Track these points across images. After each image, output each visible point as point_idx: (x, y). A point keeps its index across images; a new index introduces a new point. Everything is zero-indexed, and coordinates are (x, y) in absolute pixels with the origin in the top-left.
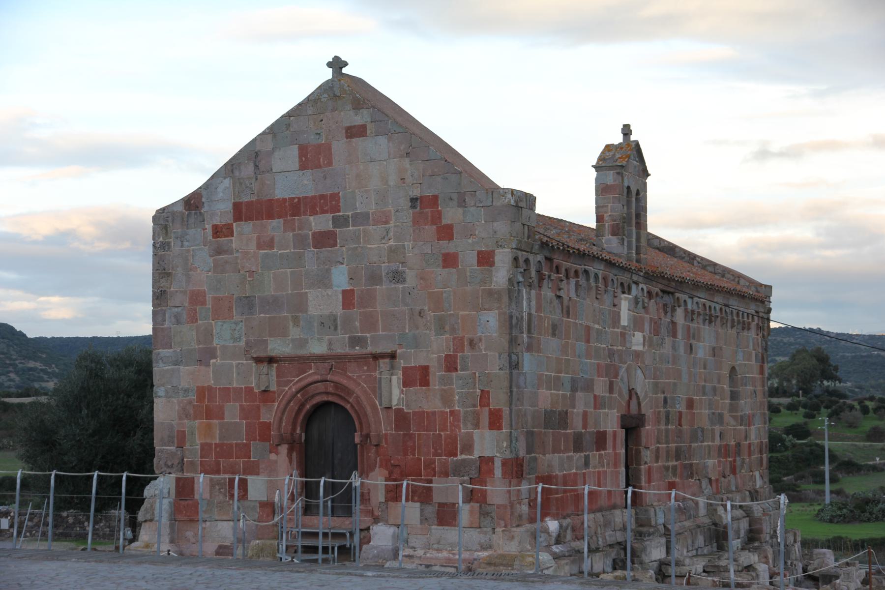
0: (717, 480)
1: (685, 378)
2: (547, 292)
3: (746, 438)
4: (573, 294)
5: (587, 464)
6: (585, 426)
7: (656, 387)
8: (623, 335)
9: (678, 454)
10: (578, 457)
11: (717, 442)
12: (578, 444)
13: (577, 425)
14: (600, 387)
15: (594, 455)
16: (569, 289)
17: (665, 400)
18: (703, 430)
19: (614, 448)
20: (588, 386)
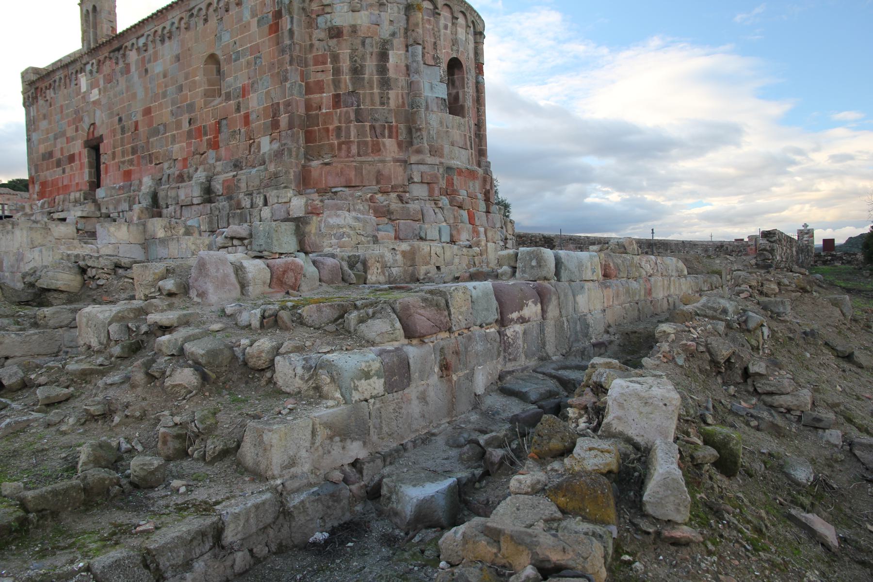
0: (185, 160)
1: (141, 94)
2: (41, 102)
3: (238, 109)
4: (53, 95)
5: (64, 172)
6: (62, 154)
7: (111, 115)
8: (83, 97)
9: (134, 151)
10: (60, 170)
11: (186, 127)
12: (59, 164)
13: (58, 155)
14: (70, 132)
15: (68, 168)
16: (50, 94)
17: (120, 120)
18: (165, 125)
19: (80, 160)
20: (63, 134)
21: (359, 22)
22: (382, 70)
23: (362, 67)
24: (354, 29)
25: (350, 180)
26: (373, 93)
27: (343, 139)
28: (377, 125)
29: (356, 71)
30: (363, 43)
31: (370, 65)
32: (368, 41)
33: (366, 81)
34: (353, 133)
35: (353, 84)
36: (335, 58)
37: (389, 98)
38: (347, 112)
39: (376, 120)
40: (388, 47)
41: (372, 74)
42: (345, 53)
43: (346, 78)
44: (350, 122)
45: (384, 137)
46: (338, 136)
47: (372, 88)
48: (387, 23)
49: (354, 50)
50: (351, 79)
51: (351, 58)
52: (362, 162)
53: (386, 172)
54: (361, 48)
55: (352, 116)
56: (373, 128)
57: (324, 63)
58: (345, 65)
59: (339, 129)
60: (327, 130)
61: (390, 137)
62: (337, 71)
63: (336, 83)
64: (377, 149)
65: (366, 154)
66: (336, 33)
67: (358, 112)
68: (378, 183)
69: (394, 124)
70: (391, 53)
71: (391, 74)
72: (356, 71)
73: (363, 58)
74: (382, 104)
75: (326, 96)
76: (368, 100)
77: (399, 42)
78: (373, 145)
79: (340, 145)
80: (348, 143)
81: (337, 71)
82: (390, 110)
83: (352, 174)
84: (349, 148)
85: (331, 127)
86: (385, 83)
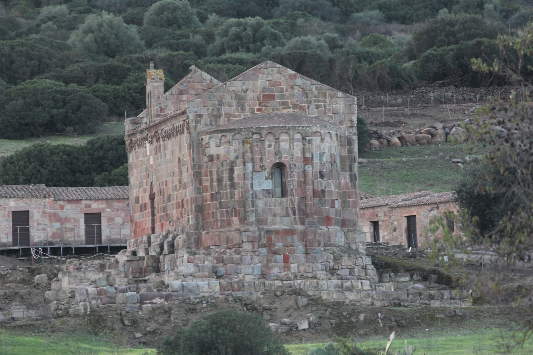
21: (220, 153)
22: (231, 178)
23: (222, 177)
24: (218, 156)
25: (215, 242)
26: (226, 193)
27: (215, 219)
28: (229, 210)
29: (220, 180)
30: (222, 164)
31: (226, 176)
32: (224, 163)
33: (224, 185)
34: (219, 215)
35: (218, 187)
36: (211, 172)
37: (234, 195)
38: (216, 204)
39: (229, 207)
40: (233, 165)
41: (226, 182)
42: (215, 169)
43: (215, 184)
44: (217, 209)
45: (232, 217)
46: (213, 217)
47: (226, 189)
48: (233, 151)
49: (218, 168)
50: (217, 185)
51: (217, 173)
52: (220, 232)
53: (231, 237)
54: (221, 168)
55: (218, 206)
56: (227, 212)
57: (207, 176)
58: (215, 177)
59: (213, 213)
60: (209, 213)
61: (235, 216)
62: (212, 181)
63: (212, 186)
64: (229, 224)
65: (224, 227)
66: (211, 159)
67: (220, 203)
68: (227, 243)
69: (237, 209)
70: (235, 168)
71: (236, 180)
72: (220, 180)
73: (222, 173)
74: (231, 198)
75: (207, 195)
76: (225, 196)
77: (239, 161)
78: (228, 221)
79: (214, 221)
80: (216, 221)
81: (212, 181)
82: (235, 201)
83: (217, 238)
84: (217, 224)
85: (210, 212)
86: (233, 186)
